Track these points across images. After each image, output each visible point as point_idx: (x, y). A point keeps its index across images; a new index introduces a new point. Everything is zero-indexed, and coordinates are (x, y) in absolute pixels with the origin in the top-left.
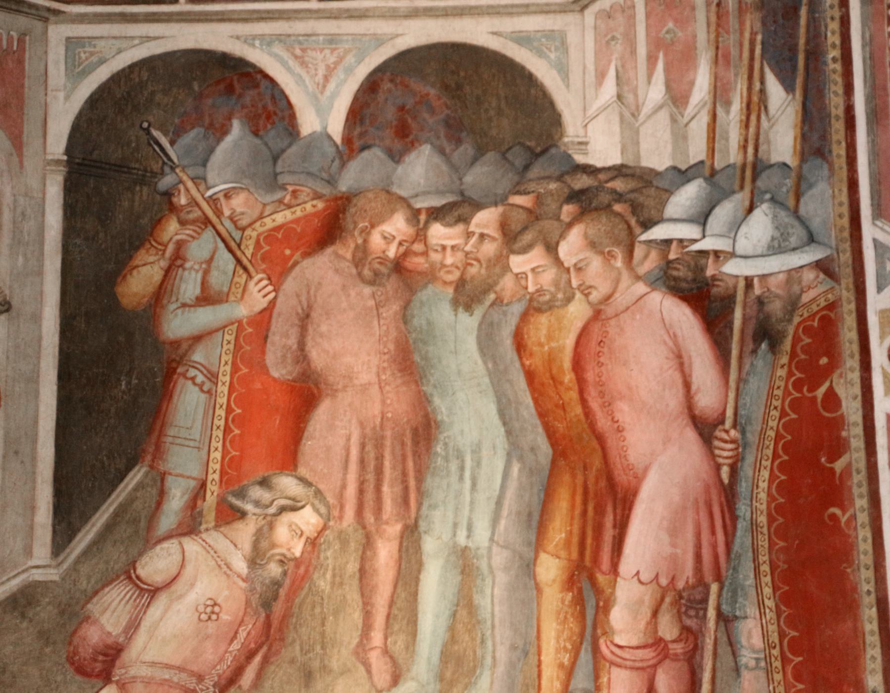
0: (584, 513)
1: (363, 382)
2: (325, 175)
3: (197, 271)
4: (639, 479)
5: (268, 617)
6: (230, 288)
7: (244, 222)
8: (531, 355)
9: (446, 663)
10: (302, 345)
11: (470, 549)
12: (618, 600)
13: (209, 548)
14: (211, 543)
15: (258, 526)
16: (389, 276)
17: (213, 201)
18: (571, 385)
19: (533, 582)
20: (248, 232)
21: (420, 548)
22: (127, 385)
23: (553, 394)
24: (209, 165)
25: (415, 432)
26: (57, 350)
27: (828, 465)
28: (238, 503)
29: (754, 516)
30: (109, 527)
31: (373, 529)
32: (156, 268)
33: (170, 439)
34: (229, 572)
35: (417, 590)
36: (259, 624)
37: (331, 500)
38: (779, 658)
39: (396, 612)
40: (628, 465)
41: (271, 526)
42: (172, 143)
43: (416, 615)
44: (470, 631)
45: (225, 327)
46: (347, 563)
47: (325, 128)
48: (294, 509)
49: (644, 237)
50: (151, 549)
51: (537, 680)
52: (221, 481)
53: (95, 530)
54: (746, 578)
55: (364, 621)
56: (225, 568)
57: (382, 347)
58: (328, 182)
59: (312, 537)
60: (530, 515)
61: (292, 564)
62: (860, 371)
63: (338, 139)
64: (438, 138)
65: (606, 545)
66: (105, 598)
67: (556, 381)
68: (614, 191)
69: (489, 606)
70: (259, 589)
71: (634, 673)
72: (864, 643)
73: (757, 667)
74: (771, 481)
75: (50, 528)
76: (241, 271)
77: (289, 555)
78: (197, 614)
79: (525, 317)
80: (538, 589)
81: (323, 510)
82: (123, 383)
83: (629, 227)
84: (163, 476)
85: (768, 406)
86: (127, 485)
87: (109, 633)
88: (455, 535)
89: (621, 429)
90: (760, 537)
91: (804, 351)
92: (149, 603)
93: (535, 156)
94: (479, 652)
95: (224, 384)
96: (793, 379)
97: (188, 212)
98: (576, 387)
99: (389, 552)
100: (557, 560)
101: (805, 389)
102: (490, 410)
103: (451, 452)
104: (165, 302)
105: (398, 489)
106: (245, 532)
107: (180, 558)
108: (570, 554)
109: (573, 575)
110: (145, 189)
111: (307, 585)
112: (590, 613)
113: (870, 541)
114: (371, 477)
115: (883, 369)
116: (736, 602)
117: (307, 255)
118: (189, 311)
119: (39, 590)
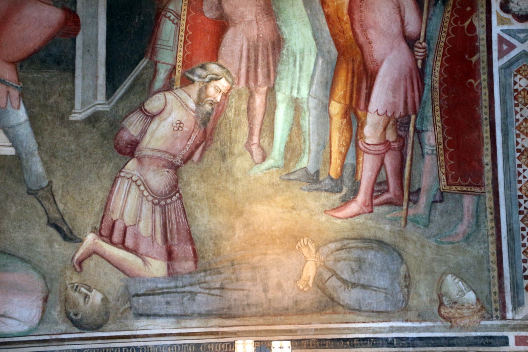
0: (353, 82)
1: (249, 20)
4: (379, 66)
5: (205, 129)
8: (328, 7)
9: (288, 151)
11: (299, 99)
12: (368, 123)
13: (177, 97)
14: (179, 95)
15: (200, 87)
18: (347, 21)
19: (328, 114)
22: (138, 20)
23: (339, 26)
25: (273, 43)
27: (469, 59)
28: (191, 76)
29: (433, 83)
30: (132, 87)
31: (253, 89)
33: (159, 46)
34: (187, 108)
35: (274, 117)
36: (201, 132)
37: (234, 75)
38: (443, 150)
39: (264, 128)
40: (374, 59)
41: (206, 87)
43: (274, 129)
44: (298, 137)
46: (242, 105)
48: (217, 79)
50: (151, 97)
51: (329, 159)
52: (183, 66)
53: (125, 87)
54: (428, 112)
55: (249, 131)
56: (185, 106)
57: (258, 3)
59: (225, 93)
60: (327, 83)
61: (216, 105)
62: (486, 14)
65: (363, 97)
66: (131, 119)
67: (340, 19)
69: (307, 126)
70: (201, 116)
71: (375, 156)
72: (483, 142)
73: (432, 154)
74: (441, 67)
75: (105, 87)
77: (214, 101)
78: (173, 127)
80: (330, 117)
81: (230, 80)
82: (137, 19)
84: (156, 63)
85: (441, 31)
86: (139, 67)
87: (133, 135)
88: (291, 92)
89: (370, 42)
90: (435, 93)
91: (459, 4)
92: (151, 122)
94: (303, 147)
95: (183, 20)
96: (453, 18)
98: (349, 22)
99: (261, 100)
100: (339, 104)
101: (459, 23)
102: (309, 33)
105: (265, 70)
106: (194, 90)
107: (164, 101)
108: (345, 101)
109: (347, 111)
112: (354, 128)
113: (487, 95)
114: (252, 65)
115: (497, 12)
116: (423, 124)
119: (100, 115)
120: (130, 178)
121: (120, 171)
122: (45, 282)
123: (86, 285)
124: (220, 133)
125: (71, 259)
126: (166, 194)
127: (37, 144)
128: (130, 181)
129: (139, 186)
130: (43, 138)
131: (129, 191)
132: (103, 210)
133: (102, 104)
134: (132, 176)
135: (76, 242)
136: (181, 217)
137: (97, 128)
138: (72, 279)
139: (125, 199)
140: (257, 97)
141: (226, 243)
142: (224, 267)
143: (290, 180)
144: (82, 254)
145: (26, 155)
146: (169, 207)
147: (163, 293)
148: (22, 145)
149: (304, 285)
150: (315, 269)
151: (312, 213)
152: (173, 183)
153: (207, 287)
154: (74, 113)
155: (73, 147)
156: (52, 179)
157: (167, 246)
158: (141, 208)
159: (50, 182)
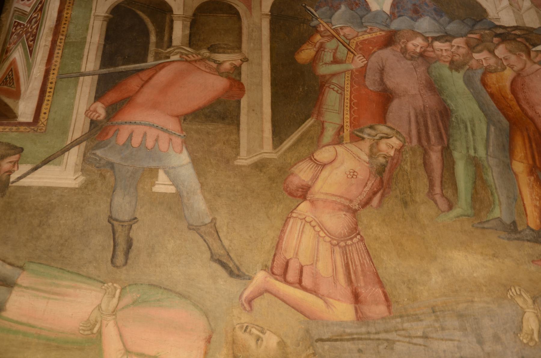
0: (531, 146)
2: (383, 24)
3: (331, 53)
5: (381, 179)
6: (346, 59)
7: (350, 37)
10: (382, 79)
11: (477, 157)
13: (348, 150)
14: (349, 148)
16: (418, 58)
17: (335, 30)
18: (512, 99)
20: (352, 41)
21: (452, 156)
24: (332, 18)
25: (441, 113)
26: (270, 76)
31: (427, 148)
32: (312, 50)
34: (359, 159)
37: (404, 135)
39: (445, 180)
41: (377, 144)
42: (316, 11)
43: (456, 182)
45: (345, 72)
47: (382, 9)
48: (388, 138)
49: (534, 49)
51: (524, 211)
52: (351, 126)
56: (357, 158)
57: (419, 82)
58: (386, 26)
59: (398, 149)
60: (504, 146)
61: (390, 159)
63: (389, 13)
64: (432, 15)
66: (300, 167)
67: (505, 98)
68: (515, 35)
69: (492, 181)
70: (375, 167)
75: (271, 139)
76: (351, 53)
77: (388, 155)
78: (346, 175)
79: (484, 74)
80: (516, 175)
81: (401, 139)
82: (301, 89)
83: (526, 46)
84: (323, 123)
86: (306, 125)
88: (468, 151)
92: (322, 170)
93: (476, 22)
94: (491, 198)
97: (325, 33)
98: (515, 100)
100: (522, 164)
102: (476, 107)
103: (459, 120)
104: (317, 62)
106: (366, 145)
107: (334, 153)
108: (528, 161)
110: (305, 25)
111: (399, 167)
114: (423, 128)
117: (380, 49)
118: (328, 66)
120: (303, 219)
121: (292, 212)
122: (208, 320)
123: (257, 326)
124: (398, 182)
125: (238, 297)
126: (345, 236)
127: (200, 184)
128: (304, 221)
129: (314, 227)
130: (206, 179)
131: (303, 231)
132: (274, 249)
133: (270, 153)
134: (306, 217)
135: (244, 279)
136: (365, 259)
137: (265, 173)
138: (240, 319)
139: (299, 239)
140: (432, 154)
141: (422, 288)
142: (423, 313)
143: (484, 228)
144: (251, 292)
145: (188, 194)
146: (350, 248)
147: (353, 339)
148: (183, 184)
149: (528, 339)
150: (537, 322)
151: (518, 262)
152: (352, 225)
153: (407, 335)
154: (240, 159)
155: (239, 187)
156: (216, 216)
157: (353, 289)
158: (318, 248)
159: (214, 219)
